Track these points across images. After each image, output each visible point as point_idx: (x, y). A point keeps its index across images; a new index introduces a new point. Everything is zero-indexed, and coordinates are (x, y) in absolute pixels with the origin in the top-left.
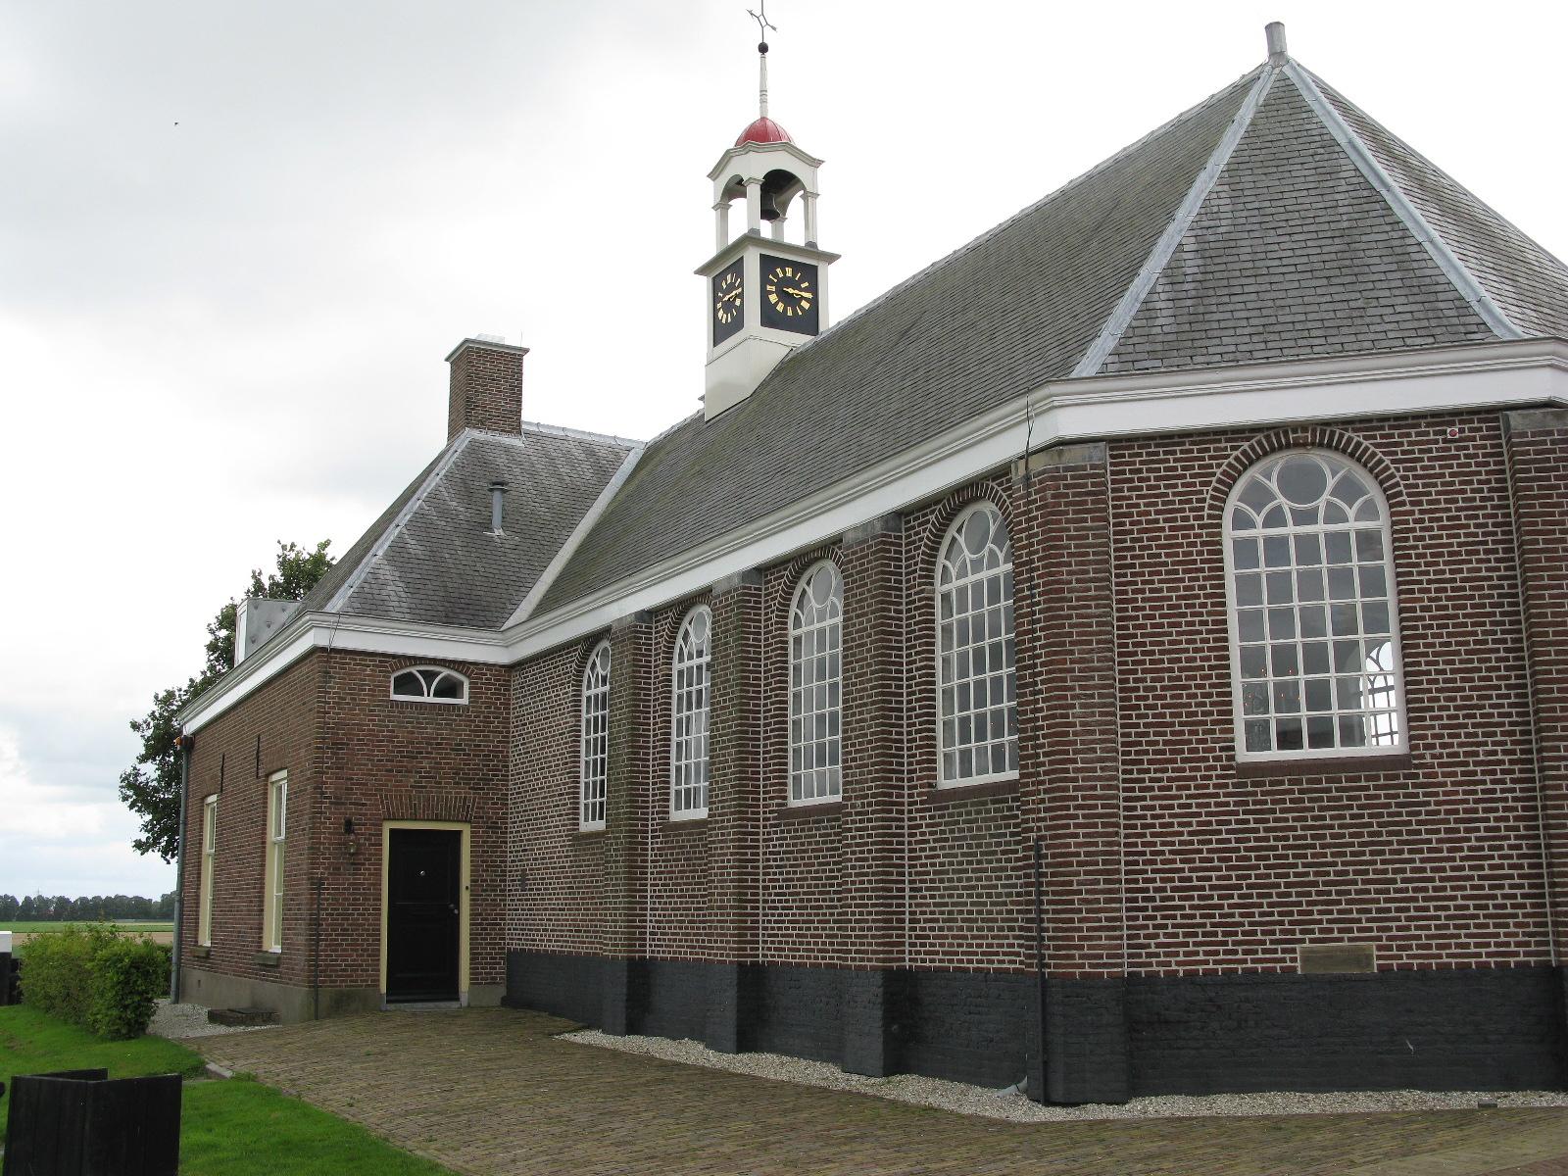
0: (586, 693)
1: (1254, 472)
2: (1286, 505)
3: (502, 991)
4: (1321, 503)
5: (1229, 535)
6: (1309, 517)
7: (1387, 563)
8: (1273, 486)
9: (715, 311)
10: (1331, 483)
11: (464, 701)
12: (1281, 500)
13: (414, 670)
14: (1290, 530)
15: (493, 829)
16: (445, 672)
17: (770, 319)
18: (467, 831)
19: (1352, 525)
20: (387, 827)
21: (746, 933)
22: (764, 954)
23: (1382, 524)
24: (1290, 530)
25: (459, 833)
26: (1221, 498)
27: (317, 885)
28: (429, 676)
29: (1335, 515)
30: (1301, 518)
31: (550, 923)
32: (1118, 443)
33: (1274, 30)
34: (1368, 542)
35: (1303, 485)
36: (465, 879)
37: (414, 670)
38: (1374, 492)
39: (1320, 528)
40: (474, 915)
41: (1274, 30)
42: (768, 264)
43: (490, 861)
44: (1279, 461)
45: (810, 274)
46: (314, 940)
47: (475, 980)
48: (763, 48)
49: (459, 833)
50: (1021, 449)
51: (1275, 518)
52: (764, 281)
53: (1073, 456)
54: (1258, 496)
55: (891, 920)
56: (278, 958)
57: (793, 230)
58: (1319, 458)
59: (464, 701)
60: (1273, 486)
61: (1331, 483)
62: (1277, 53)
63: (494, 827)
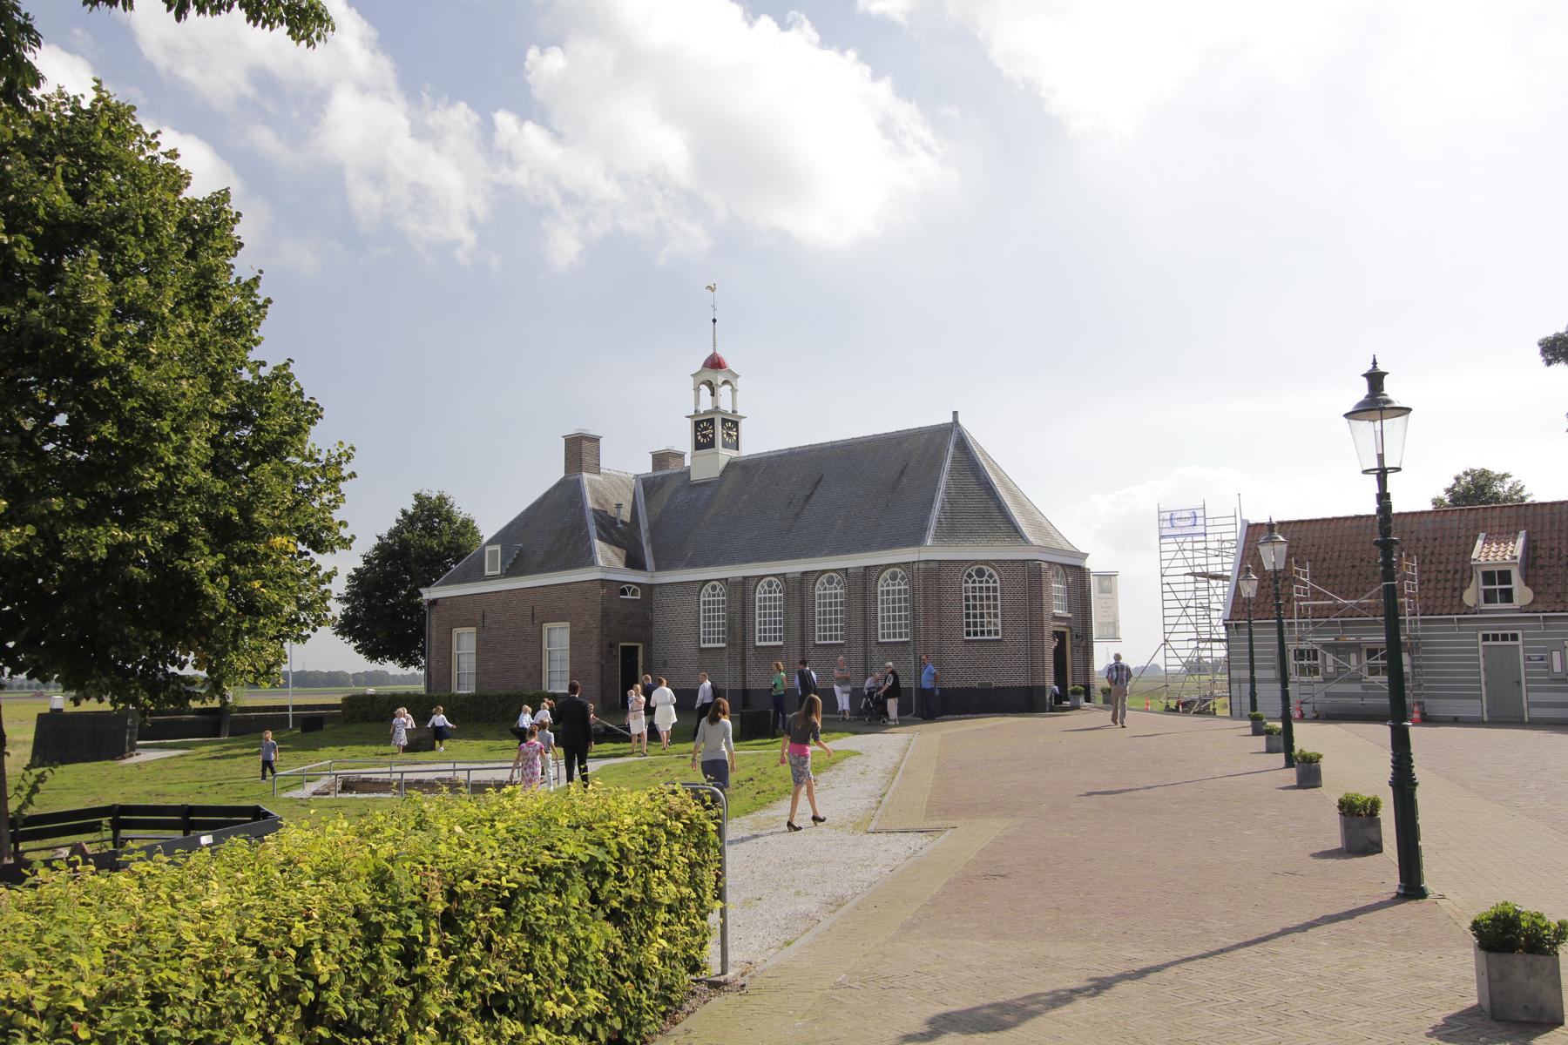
15: (648, 645)
33: (955, 413)
34: (995, 589)
36: (640, 663)
54: (970, 576)
57: (725, 404)
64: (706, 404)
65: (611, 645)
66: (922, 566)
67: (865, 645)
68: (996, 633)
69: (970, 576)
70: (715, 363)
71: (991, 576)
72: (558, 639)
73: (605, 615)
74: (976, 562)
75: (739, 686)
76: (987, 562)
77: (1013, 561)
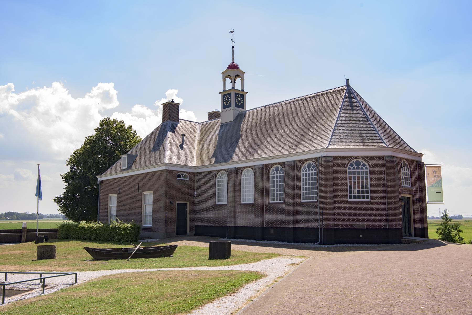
1: (351, 162)
3: (194, 233)
4: (360, 167)
5: (348, 170)
6: (358, 169)
7: (369, 175)
8: (354, 164)
9: (223, 102)
10: (362, 164)
11: (188, 179)
12: (355, 166)
13: (180, 173)
14: (356, 170)
15: (193, 202)
16: (185, 174)
17: (236, 106)
18: (188, 203)
19: (364, 170)
20: (177, 202)
21: (263, 222)
22: (266, 225)
23: (368, 170)
24: (356, 170)
25: (186, 204)
26: (347, 165)
27: (166, 213)
28: (182, 175)
29: (362, 168)
30: (357, 169)
31: (210, 220)
33: (347, 81)
37: (180, 173)
38: (367, 166)
39: (360, 170)
40: (190, 219)
41: (347, 81)
42: (236, 94)
43: (192, 209)
44: (355, 160)
45: (243, 96)
46: (166, 223)
47: (190, 231)
48: (233, 47)
49: (186, 204)
50: (320, 156)
51: (354, 168)
52: (235, 98)
53: (328, 159)
55: (294, 221)
56: (152, 227)
57: (238, 86)
58: (360, 160)
59: (188, 179)
60: (354, 164)
61: (362, 164)
62: (348, 85)
63: (193, 203)
64: (229, 86)
65: (171, 203)
66: (323, 159)
67: (294, 203)
68: (367, 197)
69: (352, 165)
70: (233, 67)
71: (364, 165)
72: (148, 199)
73: (168, 188)
74: (355, 157)
75: (232, 225)
76: (361, 157)
77: (377, 157)
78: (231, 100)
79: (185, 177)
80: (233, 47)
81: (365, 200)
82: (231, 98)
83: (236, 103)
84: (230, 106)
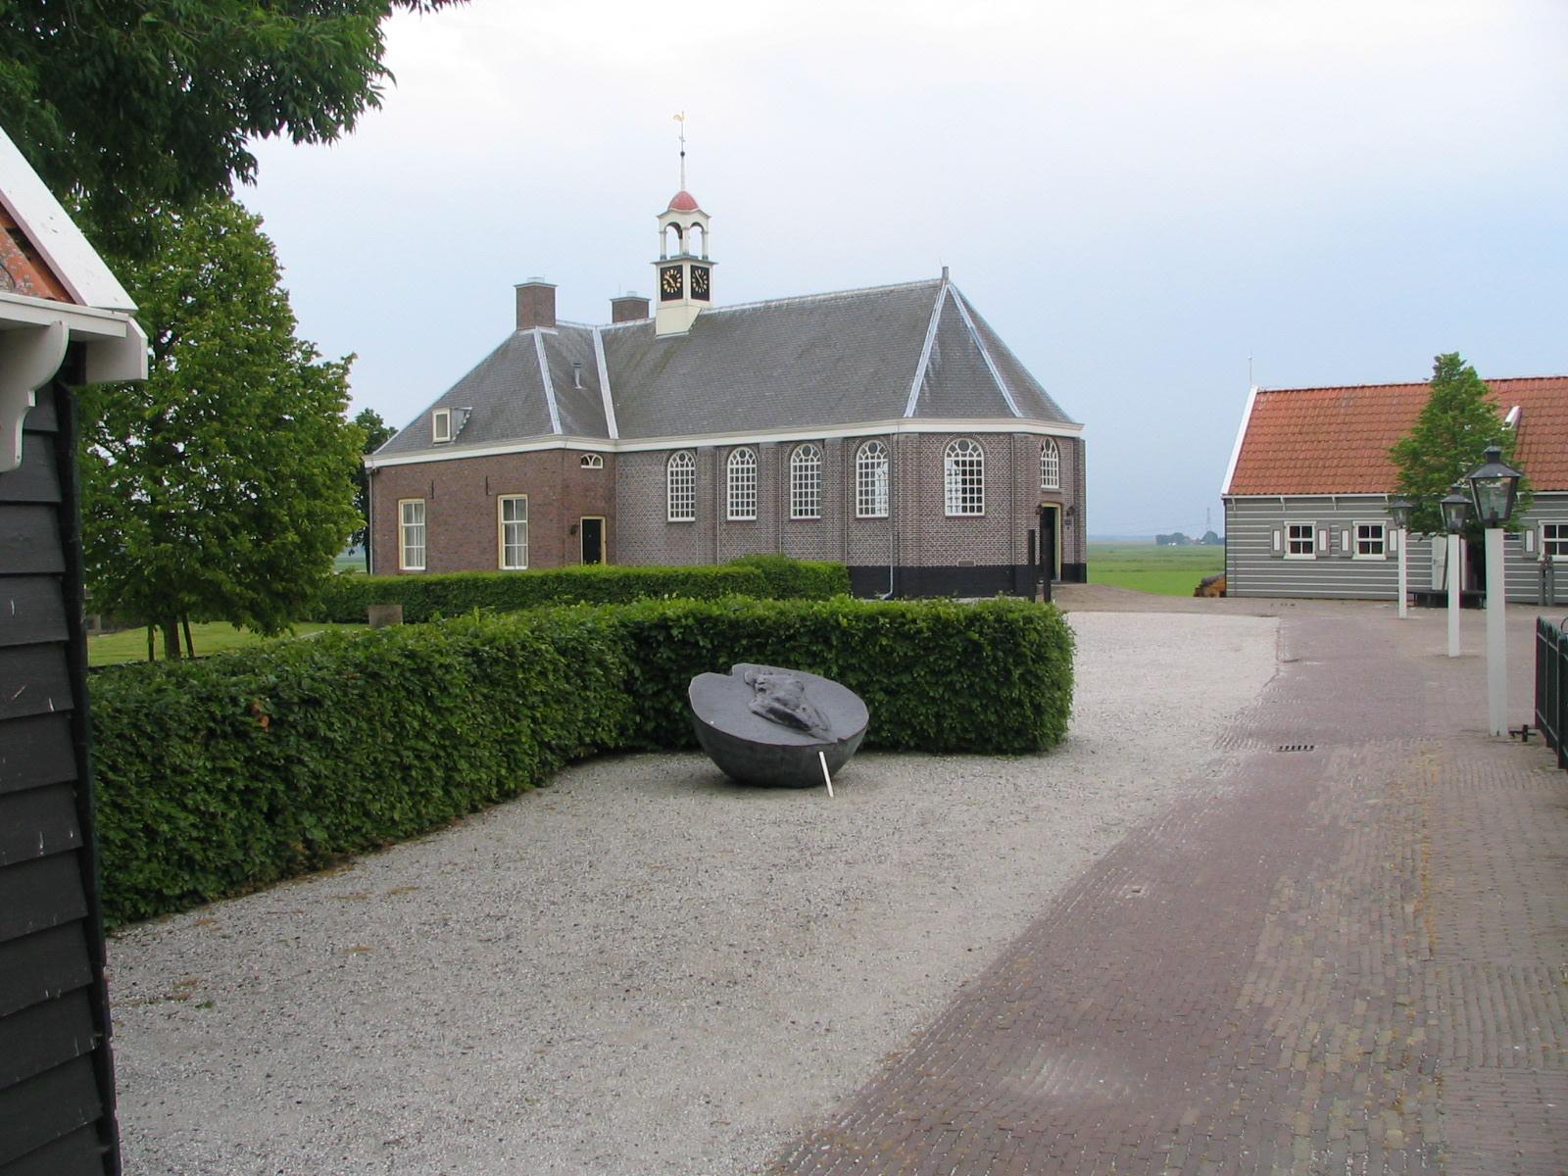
0: (669, 469)
2: (960, 452)
9: (662, 285)
13: (586, 455)
15: (611, 518)
16: (596, 456)
17: (695, 295)
23: (982, 458)
25: (600, 521)
29: (971, 455)
32: (921, 434)
34: (979, 463)
35: (964, 446)
37: (586, 455)
38: (981, 450)
43: (611, 533)
45: (706, 272)
48: (683, 154)
49: (600, 521)
58: (969, 440)
64: (673, 249)
68: (979, 509)
76: (970, 435)
78: (681, 283)
79: (596, 462)
80: (683, 154)
81: (976, 514)
82: (681, 277)
83: (693, 289)
84: (678, 294)
